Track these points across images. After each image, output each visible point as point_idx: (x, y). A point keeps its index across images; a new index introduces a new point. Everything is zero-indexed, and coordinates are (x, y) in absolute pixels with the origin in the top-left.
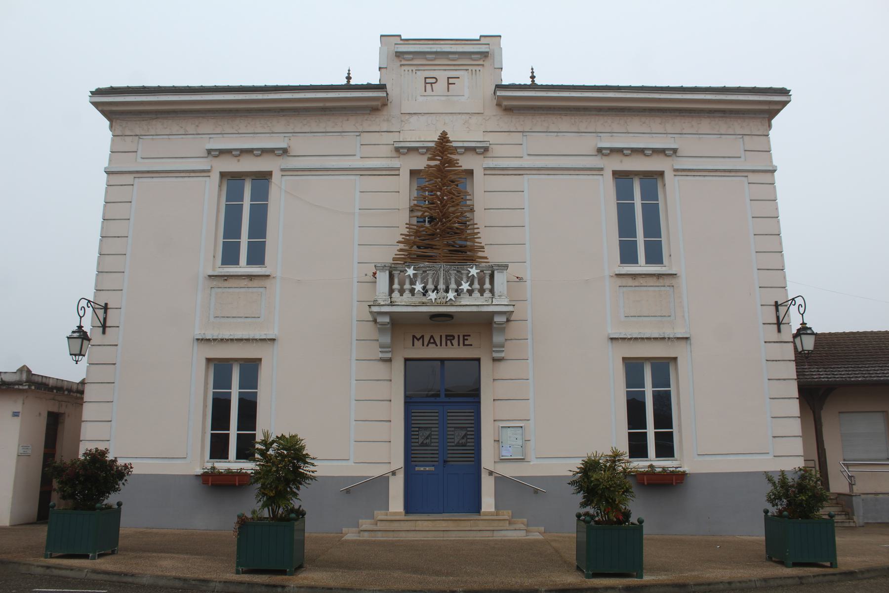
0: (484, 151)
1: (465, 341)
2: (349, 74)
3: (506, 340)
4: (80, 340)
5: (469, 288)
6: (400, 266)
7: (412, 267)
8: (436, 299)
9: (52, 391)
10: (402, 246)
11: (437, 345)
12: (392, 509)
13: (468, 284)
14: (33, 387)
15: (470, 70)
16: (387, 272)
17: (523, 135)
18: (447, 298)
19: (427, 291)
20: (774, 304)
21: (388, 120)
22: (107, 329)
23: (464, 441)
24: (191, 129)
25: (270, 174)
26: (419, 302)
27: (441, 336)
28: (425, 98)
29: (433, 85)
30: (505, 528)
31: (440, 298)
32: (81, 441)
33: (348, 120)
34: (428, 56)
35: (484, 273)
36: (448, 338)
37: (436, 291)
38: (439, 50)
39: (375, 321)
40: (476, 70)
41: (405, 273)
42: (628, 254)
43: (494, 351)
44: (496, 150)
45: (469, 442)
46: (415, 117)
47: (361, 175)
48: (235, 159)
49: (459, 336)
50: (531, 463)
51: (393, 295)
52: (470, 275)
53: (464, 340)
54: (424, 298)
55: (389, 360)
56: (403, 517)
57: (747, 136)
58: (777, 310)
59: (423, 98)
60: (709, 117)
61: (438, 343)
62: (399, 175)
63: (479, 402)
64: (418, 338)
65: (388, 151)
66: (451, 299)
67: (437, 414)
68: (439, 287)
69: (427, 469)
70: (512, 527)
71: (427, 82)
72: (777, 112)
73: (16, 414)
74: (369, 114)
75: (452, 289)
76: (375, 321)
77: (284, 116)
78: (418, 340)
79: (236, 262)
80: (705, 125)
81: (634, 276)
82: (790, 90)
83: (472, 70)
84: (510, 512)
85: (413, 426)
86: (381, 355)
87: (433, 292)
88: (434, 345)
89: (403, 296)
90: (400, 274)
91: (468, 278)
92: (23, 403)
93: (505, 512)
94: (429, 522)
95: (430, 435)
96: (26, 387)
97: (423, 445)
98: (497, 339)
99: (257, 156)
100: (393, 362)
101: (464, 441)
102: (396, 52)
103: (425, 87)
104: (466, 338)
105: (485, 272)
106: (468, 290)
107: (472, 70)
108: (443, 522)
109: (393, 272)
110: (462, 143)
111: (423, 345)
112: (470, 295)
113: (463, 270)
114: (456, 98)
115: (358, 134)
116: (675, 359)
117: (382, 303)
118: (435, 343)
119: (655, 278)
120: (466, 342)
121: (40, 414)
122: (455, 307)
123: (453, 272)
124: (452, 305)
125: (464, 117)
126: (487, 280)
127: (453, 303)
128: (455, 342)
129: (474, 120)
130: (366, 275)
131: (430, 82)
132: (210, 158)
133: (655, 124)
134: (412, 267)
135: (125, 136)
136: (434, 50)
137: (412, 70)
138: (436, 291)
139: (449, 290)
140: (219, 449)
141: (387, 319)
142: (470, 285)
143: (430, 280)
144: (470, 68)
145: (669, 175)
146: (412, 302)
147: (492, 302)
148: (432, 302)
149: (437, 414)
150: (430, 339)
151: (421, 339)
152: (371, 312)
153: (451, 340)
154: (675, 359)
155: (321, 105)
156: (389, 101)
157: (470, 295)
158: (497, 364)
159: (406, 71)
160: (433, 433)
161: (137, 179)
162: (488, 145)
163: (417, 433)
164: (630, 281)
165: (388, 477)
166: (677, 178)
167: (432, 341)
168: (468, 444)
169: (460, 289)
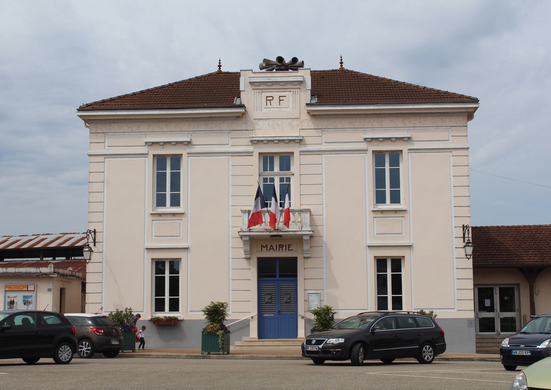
0: (300, 141)
2: (220, 63)
4: (89, 252)
9: (64, 277)
11: (274, 250)
12: (251, 336)
14: (59, 276)
15: (292, 92)
17: (322, 131)
20: (462, 226)
21: (245, 123)
22: (97, 244)
24: (135, 128)
25: (182, 155)
26: (264, 230)
27: (276, 245)
28: (267, 109)
29: (271, 101)
32: (86, 303)
33: (224, 123)
34: (268, 84)
36: (280, 246)
38: (274, 80)
39: (241, 238)
40: (295, 91)
42: (380, 198)
44: (307, 140)
45: (273, 301)
46: (261, 122)
47: (232, 156)
48: (161, 147)
49: (286, 245)
55: (249, 258)
56: (257, 340)
57: (454, 127)
58: (464, 230)
59: (266, 109)
60: (431, 116)
61: (275, 249)
62: (253, 155)
63: (297, 280)
64: (264, 246)
65: (247, 141)
71: (268, 99)
72: (474, 112)
73: (49, 290)
74: (235, 120)
77: (187, 121)
78: (264, 247)
79: (164, 205)
80: (429, 121)
81: (382, 212)
82: (479, 100)
83: (293, 92)
88: (273, 250)
92: (53, 284)
94: (271, 342)
96: (56, 276)
97: (267, 302)
98: (306, 247)
99: (174, 145)
101: (270, 301)
102: (249, 82)
103: (267, 102)
104: (290, 246)
107: (293, 92)
108: (277, 342)
110: (287, 137)
111: (267, 250)
114: (284, 109)
115: (229, 131)
116: (404, 257)
117: (245, 230)
118: (273, 249)
119: (394, 212)
120: (290, 249)
121: (58, 289)
125: (289, 120)
128: (284, 248)
129: (295, 122)
131: (269, 99)
132: (146, 147)
133: (399, 122)
135: (97, 133)
136: (271, 80)
137: (259, 92)
140: (159, 306)
141: (247, 239)
144: (292, 90)
145: (405, 153)
146: (260, 229)
149: (275, 287)
150: (271, 247)
151: (266, 247)
153: (282, 247)
154: (404, 257)
155: (208, 116)
156: (246, 112)
158: (306, 260)
159: (256, 92)
160: (273, 296)
161: (106, 159)
162: (302, 138)
163: (264, 296)
164: (380, 215)
166: (410, 154)
167: (272, 248)
168: (291, 302)
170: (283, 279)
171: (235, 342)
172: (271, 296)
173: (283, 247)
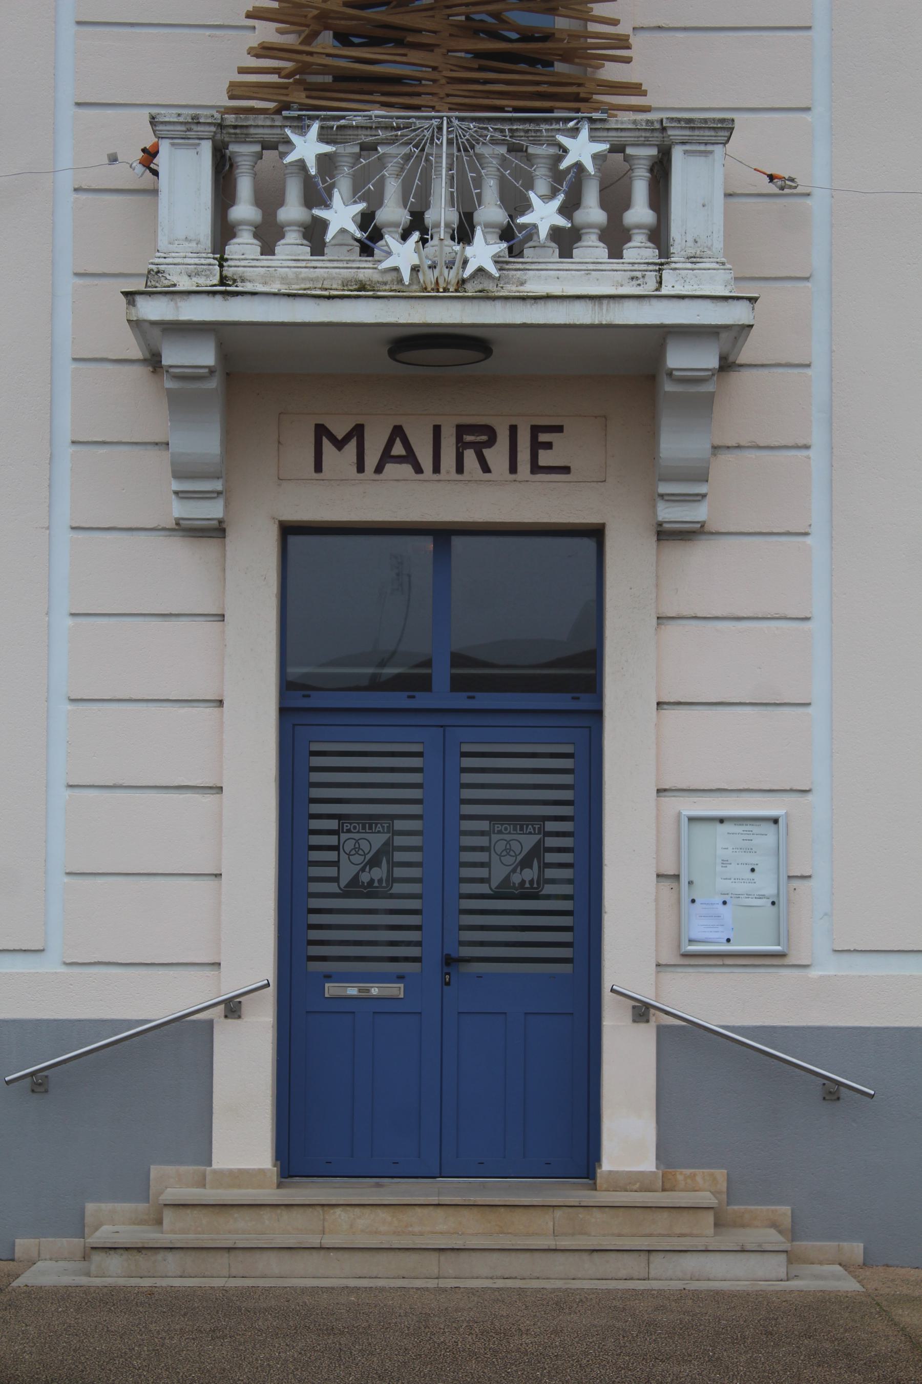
1: (542, 453)
3: (716, 448)
5: (562, 222)
6: (261, 120)
7: (315, 127)
8: (415, 269)
10: (267, 32)
11: (418, 470)
13: (556, 203)
16: (206, 148)
18: (465, 262)
19: (377, 235)
23: (529, 874)
26: (345, 284)
27: (437, 430)
30: (699, 1243)
31: (433, 267)
35: (627, 159)
36: (468, 438)
37: (416, 236)
39: (154, 361)
41: (283, 155)
43: (662, 496)
45: (553, 881)
49: (513, 430)
50: (814, 973)
51: (233, 250)
52: (564, 165)
53: (536, 446)
54: (366, 262)
56: (270, 1193)
61: (426, 461)
63: (598, 714)
64: (340, 437)
66: (480, 270)
67: (416, 762)
68: (430, 217)
69: (375, 991)
70: (730, 1240)
75: (487, 226)
76: (154, 361)
78: (340, 444)
84: (721, 1174)
85: (316, 809)
86: (179, 510)
87: (405, 237)
88: (406, 469)
89: (273, 253)
90: (260, 156)
91: (557, 176)
93: (701, 1175)
94: (382, 1214)
95: (387, 849)
97: (355, 889)
100: (228, 539)
101: (529, 874)
104: (543, 437)
105: (629, 151)
106: (556, 233)
108: (440, 1212)
109: (233, 148)
111: (361, 468)
112: (566, 253)
113: (537, 142)
117: (185, 284)
118: (410, 458)
120: (545, 458)
122: (499, 304)
123: (491, 153)
124: (485, 297)
126: (640, 190)
127: (490, 286)
128: (497, 456)
130: (113, 159)
134: (315, 127)
138: (416, 236)
139: (473, 228)
142: (567, 210)
143: (392, 188)
147: (660, 283)
148: (401, 281)
149: (416, 762)
151: (352, 447)
152: (136, 325)
157: (566, 253)
158: (676, 552)
160: (399, 841)
163: (332, 840)
165: (210, 1024)
168: (548, 889)
169: (524, 227)
170: (485, 700)
171: (90, 1207)
172: (384, 837)
173: (492, 441)
